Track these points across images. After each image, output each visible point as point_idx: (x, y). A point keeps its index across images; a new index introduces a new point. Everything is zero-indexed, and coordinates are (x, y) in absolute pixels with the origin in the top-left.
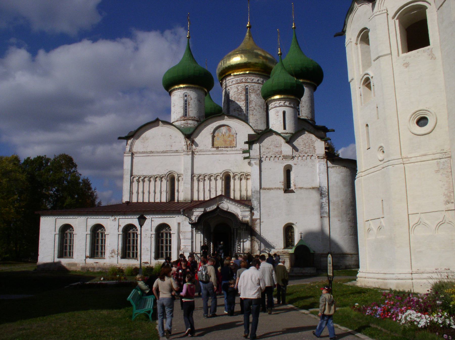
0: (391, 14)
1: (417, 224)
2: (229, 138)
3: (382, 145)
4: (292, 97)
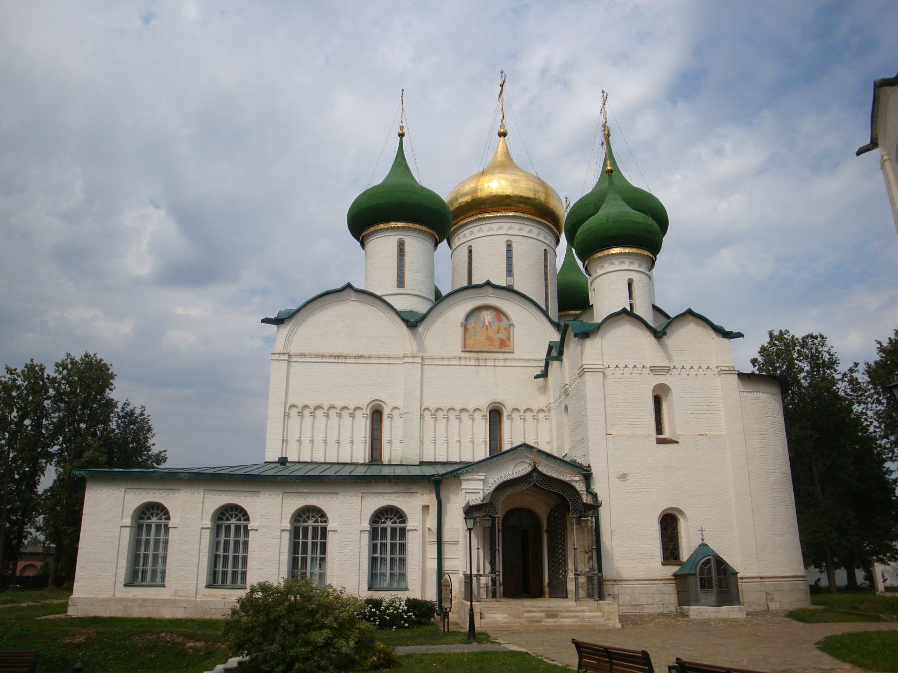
2: (499, 333)
4: (646, 253)
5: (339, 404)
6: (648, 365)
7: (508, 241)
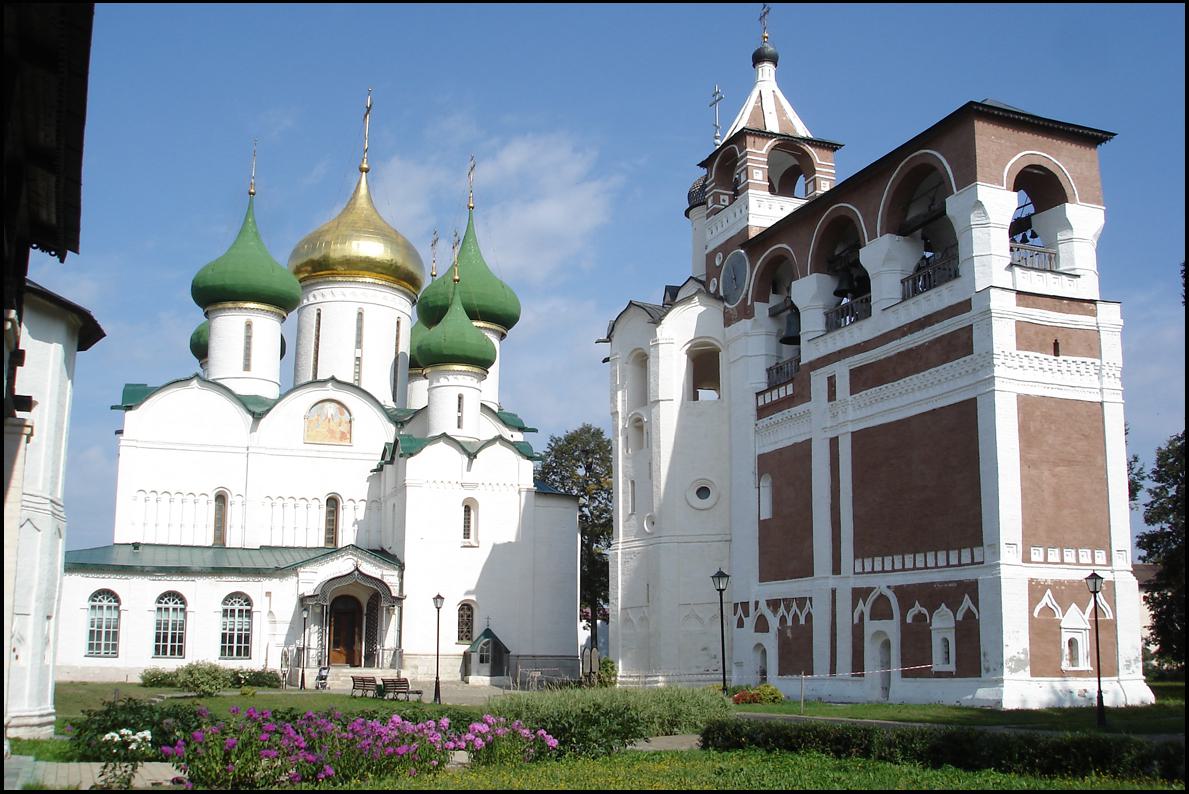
1: (687, 616)
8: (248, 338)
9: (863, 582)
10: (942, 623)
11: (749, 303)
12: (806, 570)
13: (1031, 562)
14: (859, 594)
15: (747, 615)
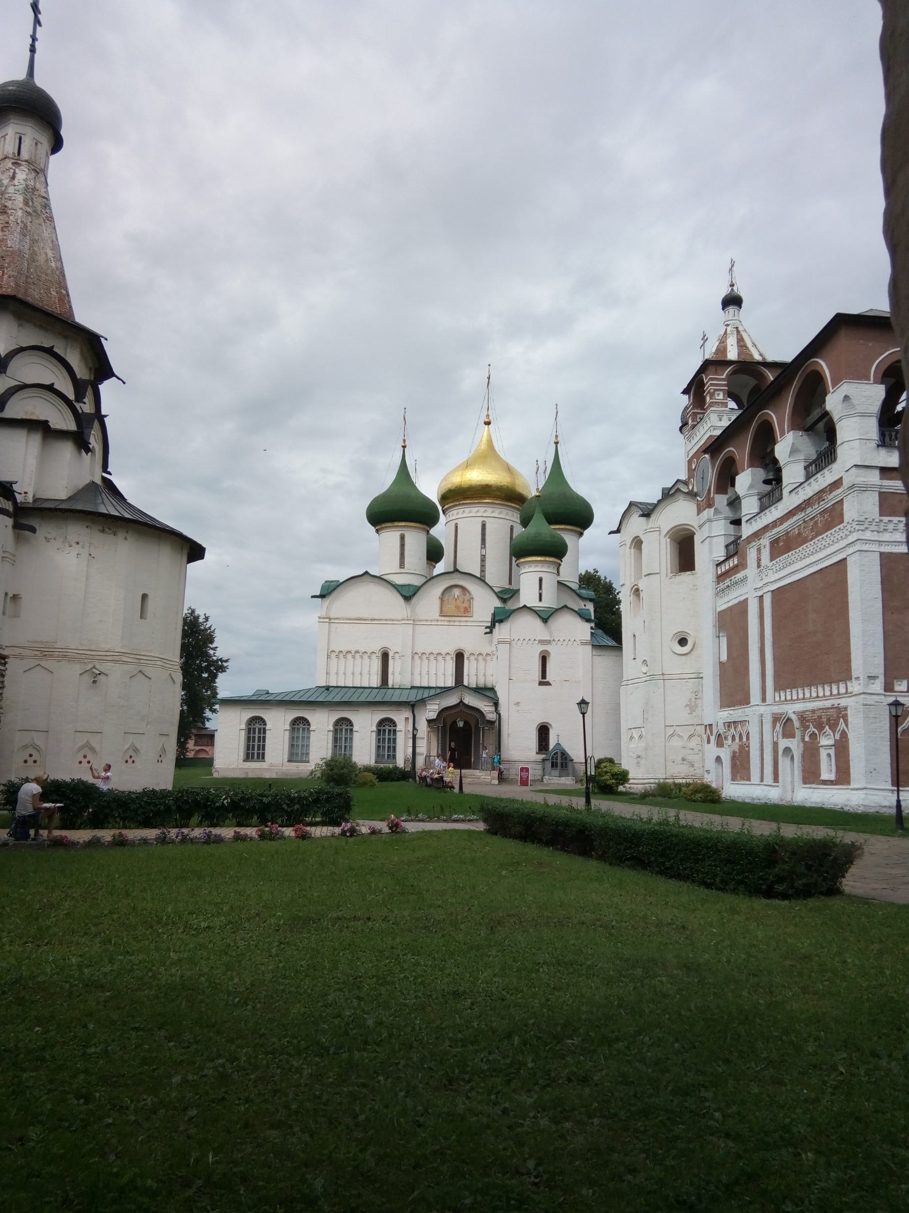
0: (664, 532)
1: (672, 735)
3: (646, 659)
5: (362, 650)
6: (537, 639)
7: (483, 521)
8: (402, 545)
9: (777, 709)
10: (826, 740)
11: (712, 496)
12: (745, 701)
13: (896, 692)
14: (776, 719)
15: (712, 735)
